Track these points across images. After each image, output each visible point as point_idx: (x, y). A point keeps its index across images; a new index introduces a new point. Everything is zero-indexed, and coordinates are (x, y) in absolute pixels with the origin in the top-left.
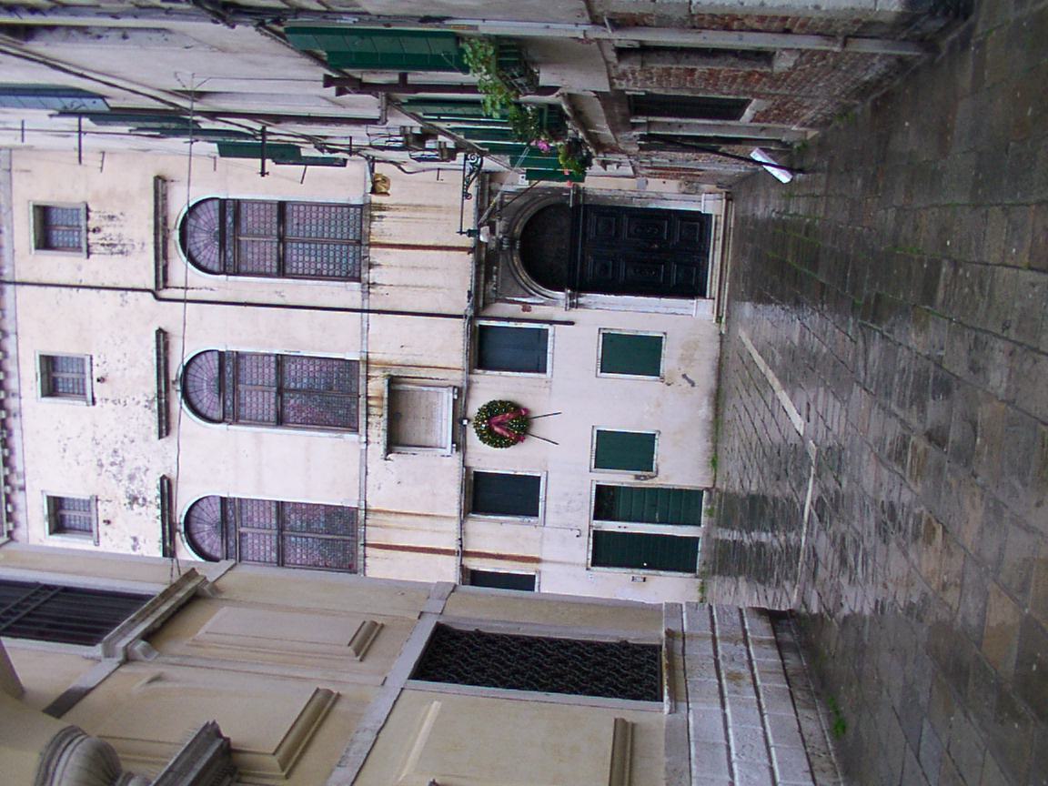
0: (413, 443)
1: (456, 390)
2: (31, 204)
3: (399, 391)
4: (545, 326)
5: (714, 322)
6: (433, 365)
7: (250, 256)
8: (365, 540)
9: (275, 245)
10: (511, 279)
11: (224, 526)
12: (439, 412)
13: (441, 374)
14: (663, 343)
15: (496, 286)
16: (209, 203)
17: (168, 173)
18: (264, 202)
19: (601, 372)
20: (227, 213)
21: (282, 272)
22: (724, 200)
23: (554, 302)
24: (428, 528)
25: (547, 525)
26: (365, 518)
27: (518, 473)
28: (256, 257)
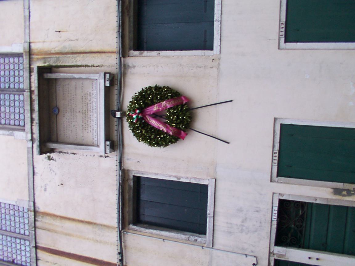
0: (71, 140)
1: (108, 76)
3: (56, 80)
6: (88, 51)
8: (36, 243)
12: (95, 104)
13: (96, 60)
25: (215, 247)
26: (35, 220)
27: (181, 181)
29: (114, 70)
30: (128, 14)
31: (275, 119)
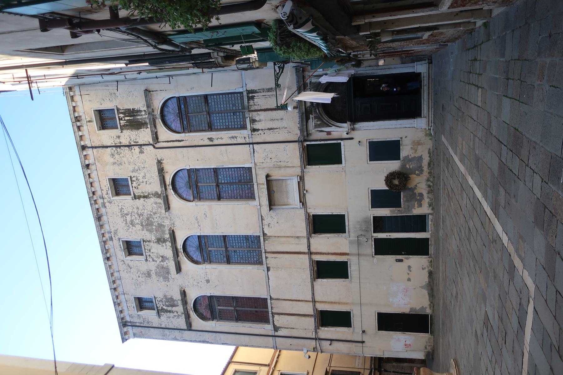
0: (282, 204)
1: (299, 177)
2: (92, 110)
4: (339, 141)
7: (194, 123)
9: (205, 116)
11: (200, 248)
14: (401, 143)
16: (172, 100)
17: (151, 88)
18: (197, 96)
19: (370, 161)
20: (181, 103)
21: (210, 128)
22: (427, 64)
24: (294, 242)
27: (333, 214)
28: (197, 123)
29: (300, 174)
31: (368, 188)
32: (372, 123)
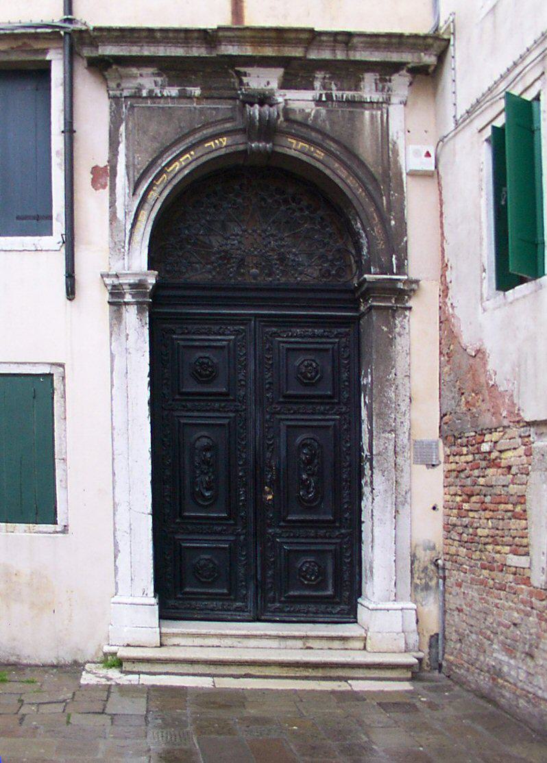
5: (107, 649)
10: (168, 131)
15: (151, 96)
23: (119, 247)
30: (12, 48)
32: (143, 393)
